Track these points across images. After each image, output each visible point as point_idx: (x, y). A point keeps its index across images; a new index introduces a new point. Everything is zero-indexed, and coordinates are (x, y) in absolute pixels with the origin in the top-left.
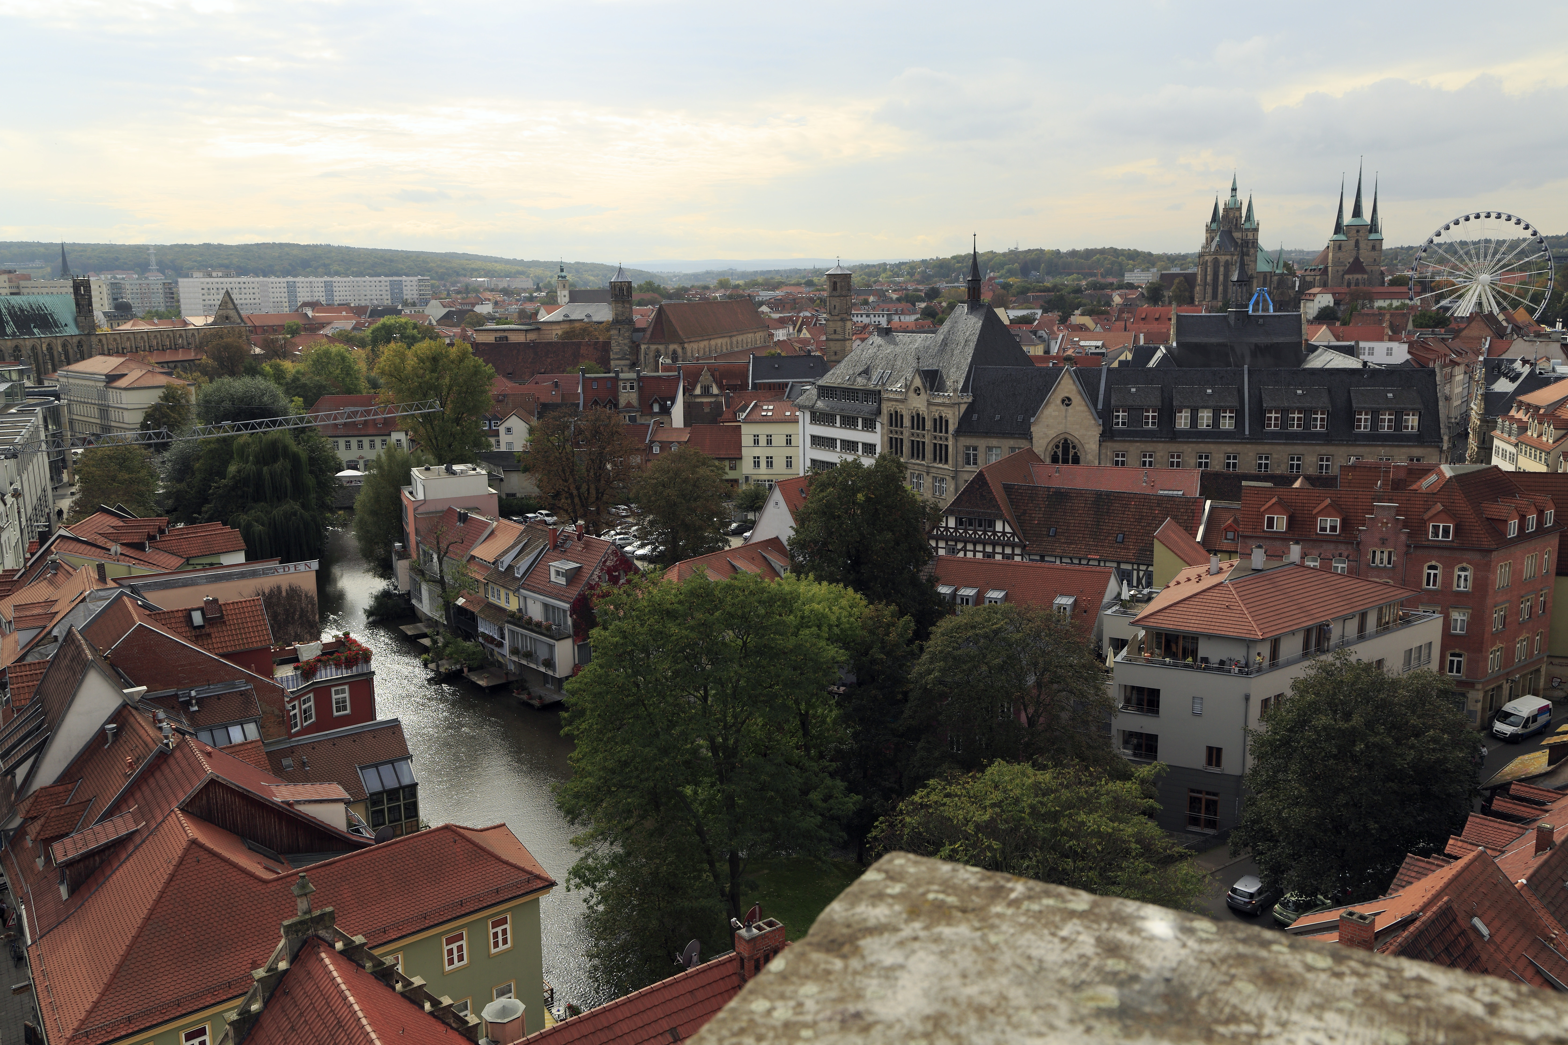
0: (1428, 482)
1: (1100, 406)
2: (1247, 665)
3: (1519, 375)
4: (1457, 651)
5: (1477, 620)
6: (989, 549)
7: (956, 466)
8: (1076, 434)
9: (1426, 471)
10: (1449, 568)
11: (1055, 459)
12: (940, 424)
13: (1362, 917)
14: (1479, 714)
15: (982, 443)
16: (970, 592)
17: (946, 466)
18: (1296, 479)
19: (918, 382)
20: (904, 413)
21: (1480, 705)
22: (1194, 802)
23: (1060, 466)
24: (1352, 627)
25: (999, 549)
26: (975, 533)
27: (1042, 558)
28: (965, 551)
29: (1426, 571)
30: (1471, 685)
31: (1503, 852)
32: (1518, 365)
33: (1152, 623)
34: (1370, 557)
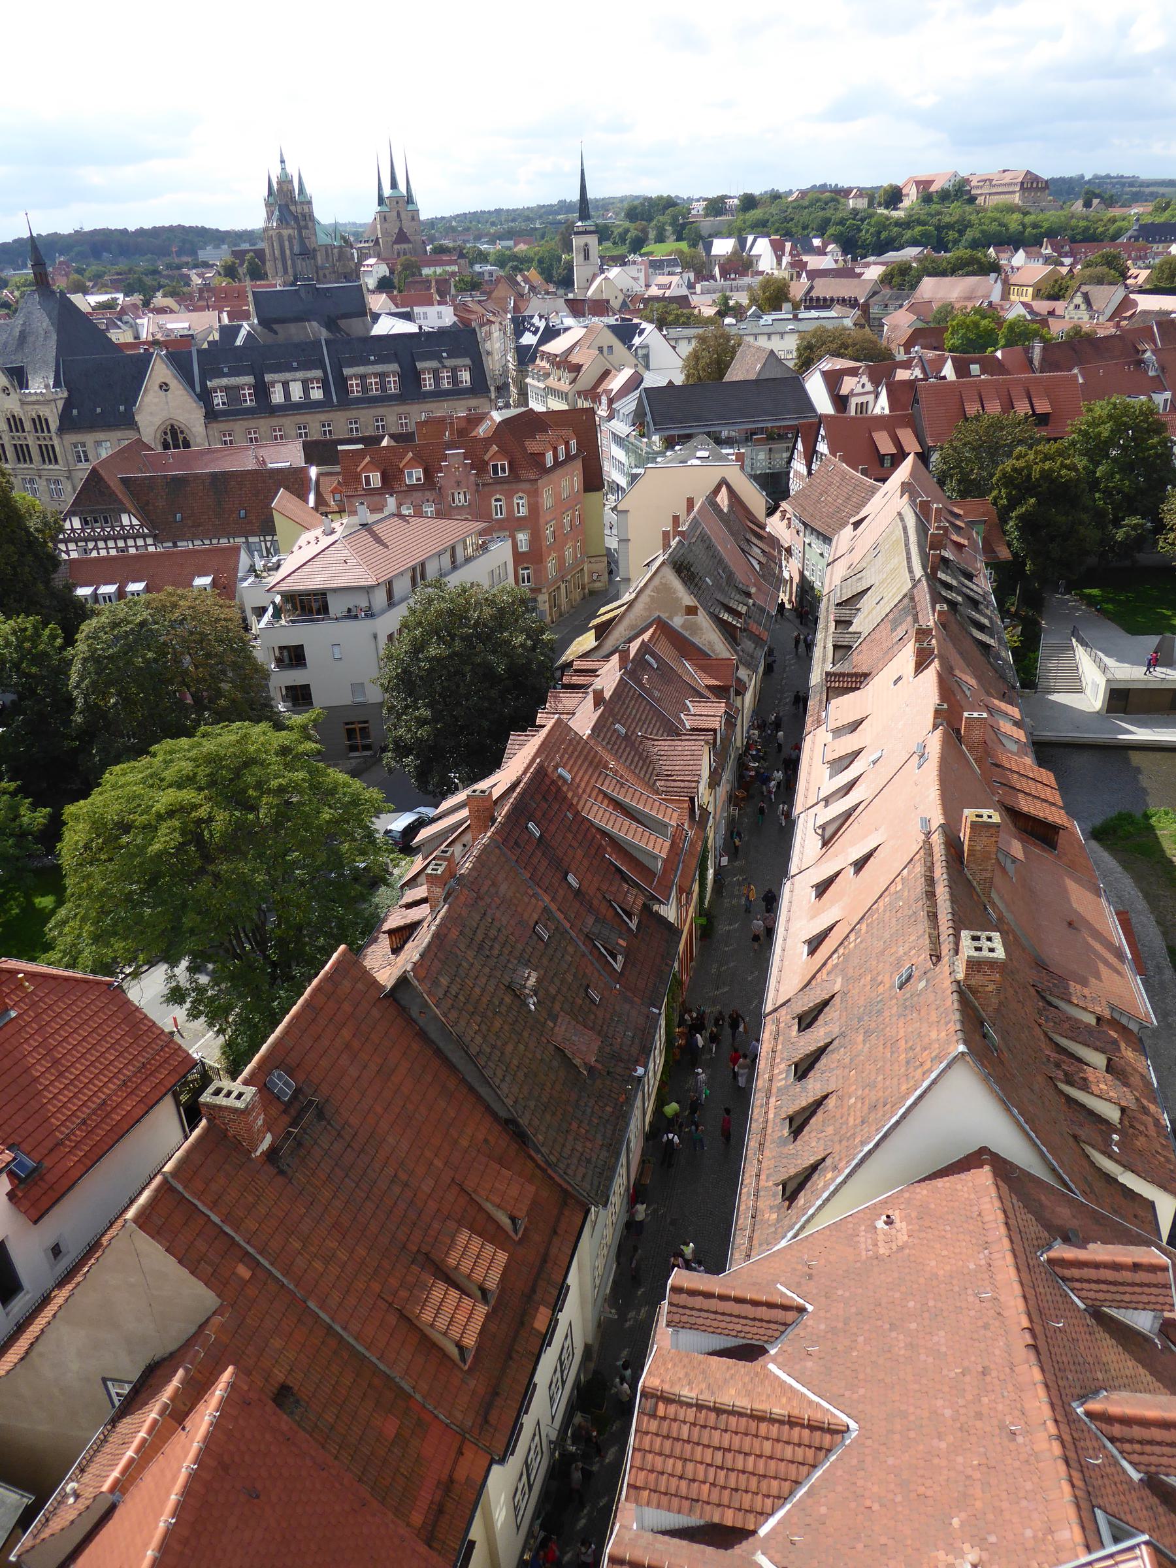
0: (482, 430)
3: (538, 329)
5: (535, 539)
6: (121, 544)
8: (180, 419)
10: (509, 498)
11: (166, 446)
12: (40, 423)
13: (483, 792)
15: (89, 438)
17: (57, 467)
18: (383, 437)
22: (350, 733)
24: (446, 560)
26: (103, 530)
28: (98, 549)
31: (574, 714)
32: (536, 320)
33: (284, 587)
34: (450, 498)
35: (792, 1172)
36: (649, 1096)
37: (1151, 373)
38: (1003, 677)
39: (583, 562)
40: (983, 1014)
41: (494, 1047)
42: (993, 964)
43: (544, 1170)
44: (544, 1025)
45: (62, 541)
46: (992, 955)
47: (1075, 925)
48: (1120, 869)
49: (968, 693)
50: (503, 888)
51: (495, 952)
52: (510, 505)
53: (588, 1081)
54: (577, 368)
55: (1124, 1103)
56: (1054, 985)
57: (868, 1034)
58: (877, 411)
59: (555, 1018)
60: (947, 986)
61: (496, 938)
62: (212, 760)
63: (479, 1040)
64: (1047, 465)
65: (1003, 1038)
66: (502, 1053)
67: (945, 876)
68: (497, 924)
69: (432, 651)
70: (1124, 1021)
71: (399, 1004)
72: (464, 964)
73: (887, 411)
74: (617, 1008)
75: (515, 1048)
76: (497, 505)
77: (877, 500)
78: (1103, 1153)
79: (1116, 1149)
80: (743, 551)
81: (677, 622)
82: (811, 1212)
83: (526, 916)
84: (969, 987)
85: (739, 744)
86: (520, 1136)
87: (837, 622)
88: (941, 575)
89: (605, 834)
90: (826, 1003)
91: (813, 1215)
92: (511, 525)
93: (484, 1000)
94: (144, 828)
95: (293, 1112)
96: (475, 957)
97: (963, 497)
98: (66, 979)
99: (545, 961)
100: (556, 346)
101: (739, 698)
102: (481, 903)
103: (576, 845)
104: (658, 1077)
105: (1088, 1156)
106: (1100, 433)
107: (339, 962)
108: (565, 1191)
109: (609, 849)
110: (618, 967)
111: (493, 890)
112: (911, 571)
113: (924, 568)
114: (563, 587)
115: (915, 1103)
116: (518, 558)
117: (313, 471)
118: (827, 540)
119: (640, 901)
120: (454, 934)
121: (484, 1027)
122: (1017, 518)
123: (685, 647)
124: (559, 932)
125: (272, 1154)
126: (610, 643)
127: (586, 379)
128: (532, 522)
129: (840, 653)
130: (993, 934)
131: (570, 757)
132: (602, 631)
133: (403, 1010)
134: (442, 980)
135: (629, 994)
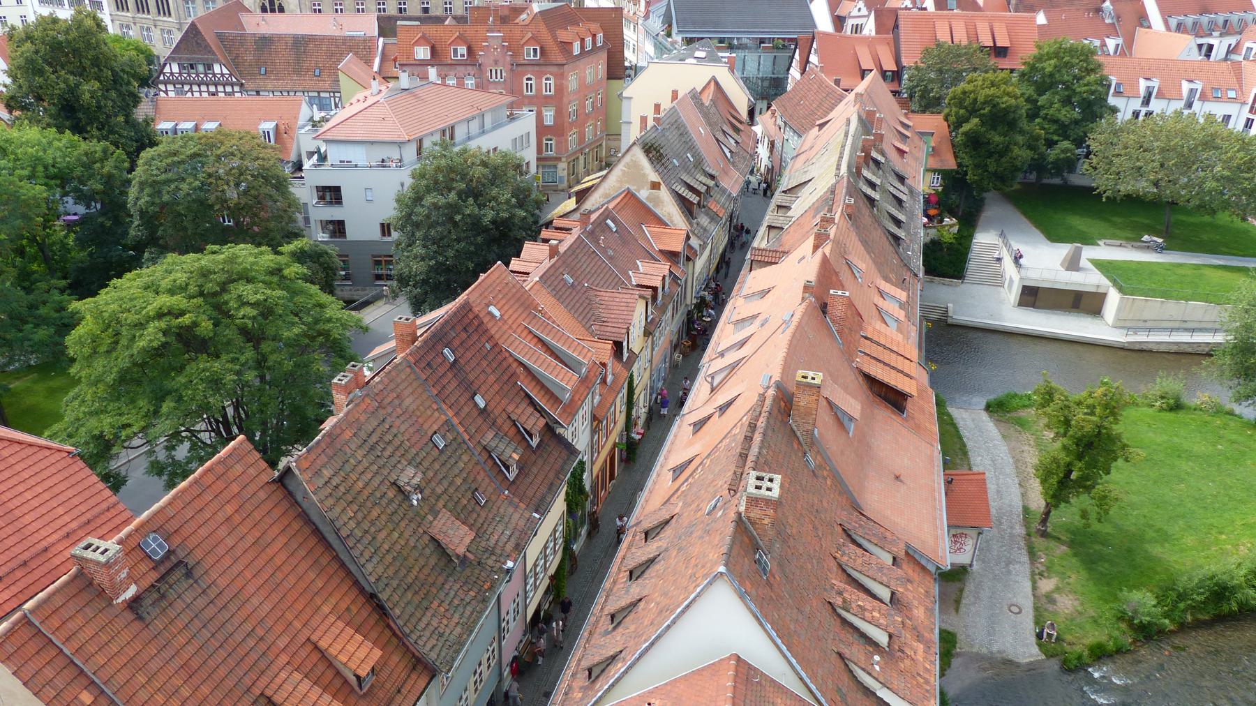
2: (401, 161)
4: (549, 137)
5: (559, 114)
6: (212, 89)
7: (180, 19)
10: (539, 78)
11: (264, 10)
14: (566, 178)
16: (189, 125)
17: (170, 19)
18: (447, 18)
21: (566, 172)
23: (269, 15)
24: (474, 126)
25: (220, 88)
27: (258, 93)
28: (192, 92)
29: (525, 82)
30: (559, 159)
35: (597, 659)
36: (536, 588)
37: (1108, 21)
41: (366, 532)
42: (767, 501)
43: (399, 639)
45: (162, 82)
47: (902, 478)
50: (408, 402)
51: (387, 453)
55: (891, 630)
56: (861, 526)
57: (680, 549)
60: (733, 516)
61: (390, 442)
62: (205, 273)
63: (352, 524)
64: (992, 91)
65: (780, 565)
67: (763, 425)
68: (394, 430)
69: (429, 200)
70: (923, 562)
71: (286, 488)
72: (352, 461)
73: (873, 33)
74: (502, 510)
75: (389, 535)
76: (531, 83)
77: (841, 106)
78: (863, 669)
79: (877, 668)
81: (643, 194)
82: (599, 694)
83: (426, 427)
84: (749, 518)
85: (688, 301)
86: (381, 610)
88: (865, 172)
89: (521, 364)
90: (667, 522)
91: (601, 697)
92: (539, 102)
93: (366, 493)
94: (136, 325)
95: (162, 570)
96: (365, 456)
97: (924, 112)
98: (31, 445)
99: (437, 466)
102: (381, 412)
104: (552, 571)
105: (851, 672)
107: (235, 449)
110: (511, 477)
111: (397, 402)
112: (838, 168)
113: (849, 167)
115: (683, 612)
116: (542, 130)
117: (381, 40)
118: (800, 136)
119: (542, 422)
120: (348, 434)
121: (360, 515)
123: (648, 215)
125: (136, 600)
128: (558, 100)
129: (773, 233)
130: (775, 476)
132: (582, 196)
134: (325, 472)
135: (516, 500)
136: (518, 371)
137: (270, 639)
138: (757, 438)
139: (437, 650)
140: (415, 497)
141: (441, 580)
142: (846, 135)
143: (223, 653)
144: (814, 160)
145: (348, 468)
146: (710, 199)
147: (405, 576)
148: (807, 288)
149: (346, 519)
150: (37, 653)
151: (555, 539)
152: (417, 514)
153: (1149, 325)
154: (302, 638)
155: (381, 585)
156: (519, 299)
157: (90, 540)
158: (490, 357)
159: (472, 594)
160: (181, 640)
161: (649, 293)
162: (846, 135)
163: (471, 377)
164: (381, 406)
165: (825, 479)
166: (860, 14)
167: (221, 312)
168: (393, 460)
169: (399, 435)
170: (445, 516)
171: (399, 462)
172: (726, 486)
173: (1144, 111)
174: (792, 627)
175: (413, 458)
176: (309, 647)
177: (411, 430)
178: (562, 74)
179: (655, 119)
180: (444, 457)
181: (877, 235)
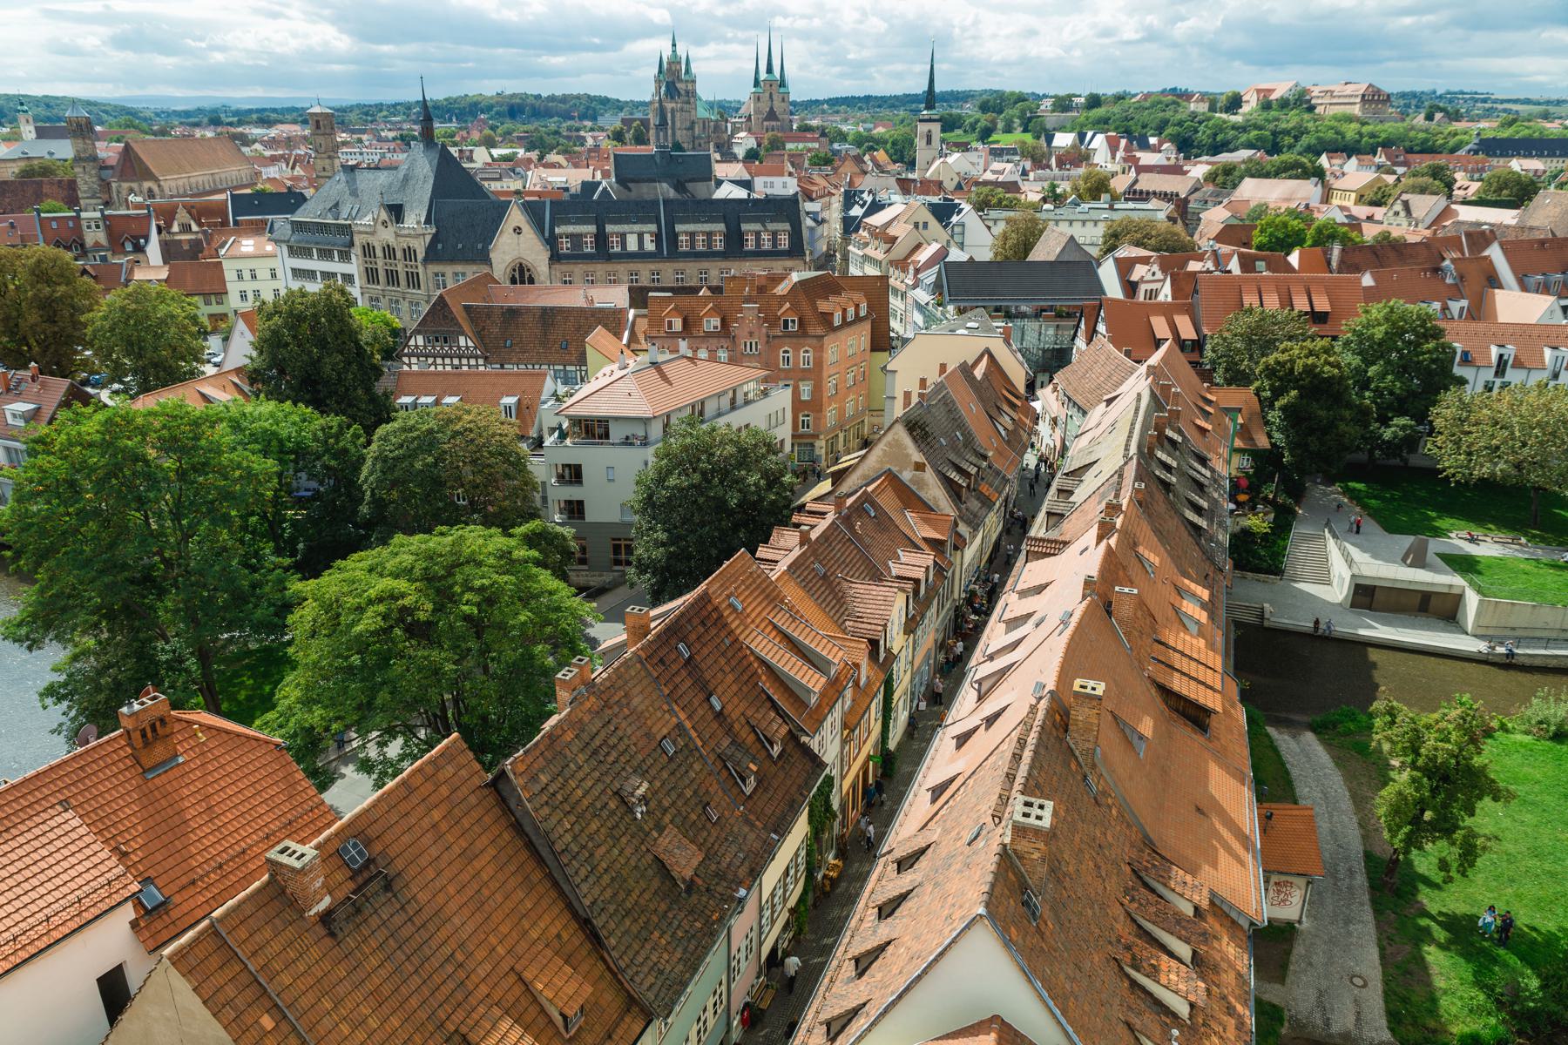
0: (782, 289)
1: (547, 234)
3: (865, 202)
6: (456, 361)
9: (781, 278)
11: (513, 281)
12: (409, 253)
15: (449, 270)
19: (384, 215)
20: (376, 245)
21: (823, 451)
22: (617, 549)
24: (725, 402)
25: (464, 361)
26: (442, 348)
30: (816, 437)
32: (865, 196)
33: (571, 412)
35: (836, 1012)
36: (773, 922)
37: (1449, 281)
38: (1209, 557)
39: (864, 414)
40: (1030, 881)
41: (584, 847)
42: (1037, 832)
44: (647, 834)
45: (406, 355)
46: (1038, 823)
48: (1331, 765)
49: (1149, 570)
50: (636, 701)
51: (611, 759)
52: (797, 357)
53: (683, 895)
54: (893, 240)
55: (1192, 998)
57: (936, 885)
58: (1161, 298)
59: (661, 829)
60: (996, 848)
61: (615, 746)
62: (430, 556)
63: (568, 838)
64: (1310, 361)
66: (591, 855)
68: (620, 733)
69: (672, 481)
70: (1233, 915)
72: (572, 765)
73: (1169, 299)
74: (735, 829)
75: (608, 852)
77: (1132, 380)
80: (991, 417)
81: (907, 476)
83: (654, 730)
84: (1015, 851)
85: (956, 596)
86: (595, 938)
87: (1060, 491)
88: (1159, 454)
89: (763, 662)
90: (923, 851)
92: (793, 376)
95: (360, 880)
96: (587, 761)
97: (1229, 384)
98: (238, 735)
99: (665, 775)
100: (877, 219)
101: (959, 552)
103: (727, 669)
104: (792, 902)
106: (1373, 335)
107: (447, 748)
108: (630, 997)
109: (764, 678)
110: (748, 790)
111: (624, 701)
113: (1140, 447)
114: (841, 436)
116: (798, 405)
117: (632, 313)
119: (784, 730)
120: (569, 736)
121: (577, 828)
122: (1280, 409)
123: (910, 498)
124: (689, 750)
125: (326, 918)
126: (845, 488)
127: (899, 251)
128: (815, 373)
129: (1053, 520)
131: (747, 588)
132: (838, 477)
133: (503, 801)
134: (542, 777)
136: (760, 671)
137: (471, 965)
138: (1027, 755)
139: (656, 988)
140: (639, 810)
141: (663, 906)
142: (1137, 410)
143: (417, 980)
144: (1100, 439)
145: (567, 773)
146: (983, 483)
147: (623, 901)
148: (1088, 583)
149: (562, 831)
150: (221, 968)
151: (797, 865)
152: (641, 829)
153: (1518, 633)
154: (505, 966)
155: (596, 909)
156: (763, 591)
157: (287, 843)
158: (729, 655)
159: (698, 925)
160: (374, 962)
161: (909, 586)
162: (1137, 410)
163: (707, 676)
164: (607, 705)
165: (1110, 807)
166: (1155, 278)
167: (445, 598)
168: (618, 767)
169: (625, 740)
170: (671, 831)
171: (624, 769)
172: (990, 812)
173: (1498, 382)
174: (1068, 986)
175: (639, 766)
176: (512, 978)
177: (638, 733)
178: (822, 346)
179: (921, 395)
180: (673, 766)
181: (1173, 524)
